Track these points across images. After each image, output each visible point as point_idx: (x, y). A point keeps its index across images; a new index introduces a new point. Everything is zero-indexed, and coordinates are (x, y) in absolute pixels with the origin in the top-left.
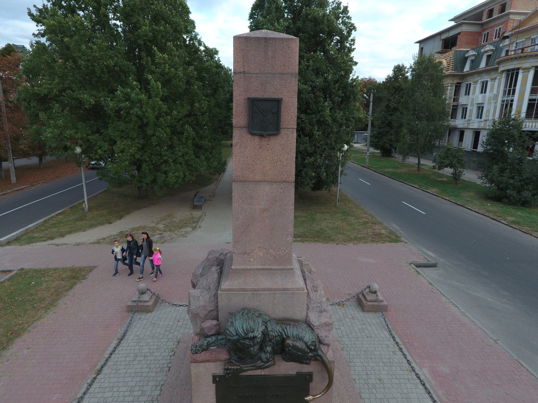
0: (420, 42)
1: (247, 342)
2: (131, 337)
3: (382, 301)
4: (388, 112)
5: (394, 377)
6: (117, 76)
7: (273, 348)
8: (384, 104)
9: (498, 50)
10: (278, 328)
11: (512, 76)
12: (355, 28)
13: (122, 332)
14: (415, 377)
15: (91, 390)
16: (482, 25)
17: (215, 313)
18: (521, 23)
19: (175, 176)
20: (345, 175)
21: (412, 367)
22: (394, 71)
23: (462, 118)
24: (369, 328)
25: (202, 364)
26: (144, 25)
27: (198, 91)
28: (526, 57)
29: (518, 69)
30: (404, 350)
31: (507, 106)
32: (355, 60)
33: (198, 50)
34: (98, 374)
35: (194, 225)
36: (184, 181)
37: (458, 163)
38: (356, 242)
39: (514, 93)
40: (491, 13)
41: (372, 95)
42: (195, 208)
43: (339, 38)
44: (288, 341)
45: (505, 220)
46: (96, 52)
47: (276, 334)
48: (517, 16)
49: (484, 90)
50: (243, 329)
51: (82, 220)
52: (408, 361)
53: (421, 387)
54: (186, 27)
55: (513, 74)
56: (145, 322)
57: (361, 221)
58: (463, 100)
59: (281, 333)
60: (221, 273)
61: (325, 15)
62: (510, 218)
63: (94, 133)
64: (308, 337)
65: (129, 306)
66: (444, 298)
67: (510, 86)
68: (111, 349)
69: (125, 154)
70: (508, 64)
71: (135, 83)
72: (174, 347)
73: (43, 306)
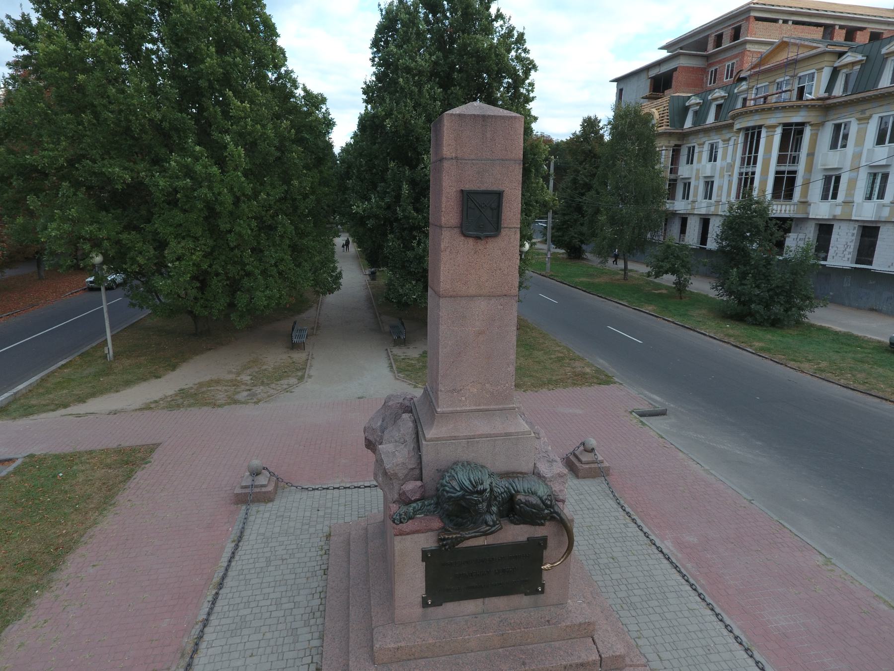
0: (618, 80)
1: (475, 497)
2: (253, 537)
3: (602, 462)
4: (576, 189)
5: (630, 553)
6: (167, 137)
7: (498, 508)
8: (568, 179)
9: (731, 98)
10: (504, 483)
11: (752, 136)
12: (535, 67)
13: (234, 533)
14: (656, 551)
15: (217, 609)
16: (707, 57)
17: (417, 472)
18: (763, 59)
19: (265, 296)
20: (526, 288)
21: (651, 540)
22: (583, 125)
23: (683, 198)
24: (589, 499)
25: (409, 537)
26: (208, 56)
27: (297, 161)
28: (770, 109)
29: (760, 127)
30: (639, 522)
31: (747, 181)
32: (533, 113)
33: (292, 95)
34: (221, 588)
35: (300, 374)
36: (278, 304)
37: (683, 266)
38: (551, 387)
39: (755, 163)
40: (719, 39)
42: (294, 346)
43: (510, 81)
44: (519, 497)
45: (751, 346)
46: (132, 97)
47: (502, 490)
48: (756, 46)
49: (713, 158)
50: (470, 481)
51: (107, 375)
52: (645, 533)
53: (666, 561)
54: (274, 58)
55: (753, 134)
56: (267, 515)
57: (553, 356)
58: (684, 171)
59: (508, 488)
60: (416, 422)
61: (492, 45)
62: (757, 344)
63: (129, 227)
64: (542, 491)
65: (237, 495)
66: (681, 454)
67: (750, 153)
68: (226, 555)
69: (183, 262)
70: (746, 119)
71: (198, 148)
72: (322, 543)
73: (93, 506)
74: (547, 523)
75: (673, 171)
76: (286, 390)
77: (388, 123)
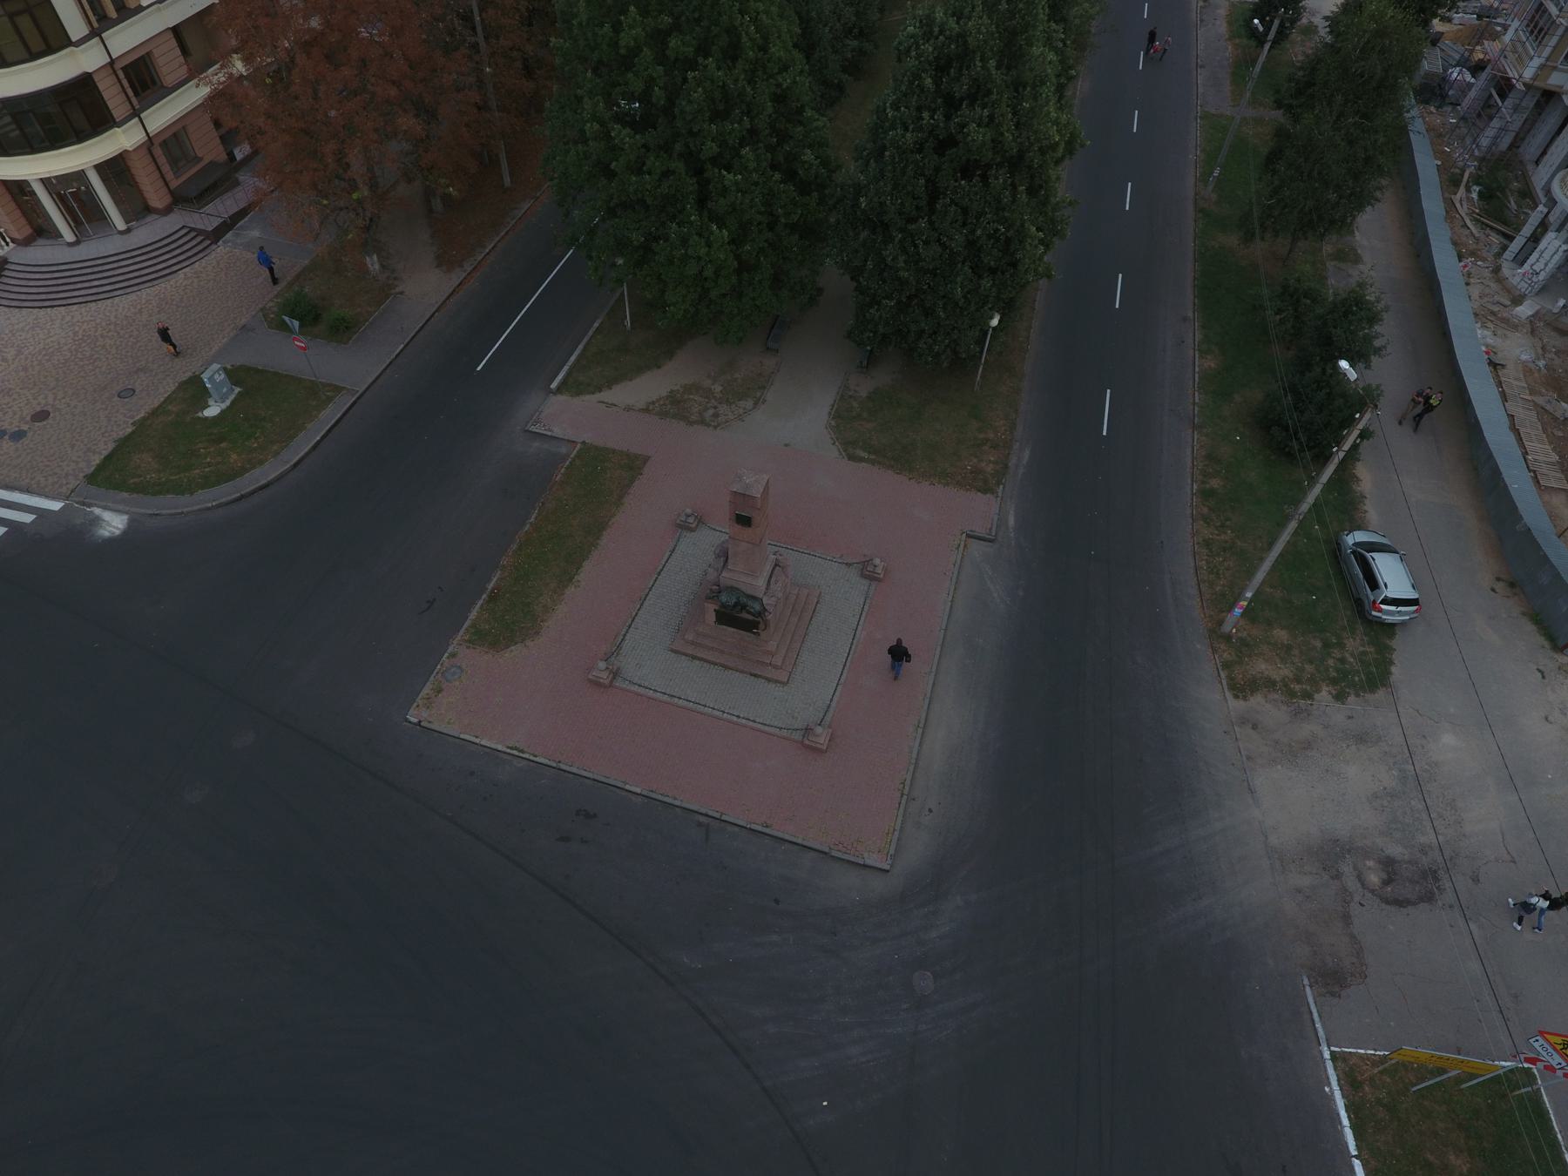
41: (1277, 22)
57: (982, 436)
62: (1215, 483)
64: (757, 607)
76: (740, 418)
77: (863, 201)
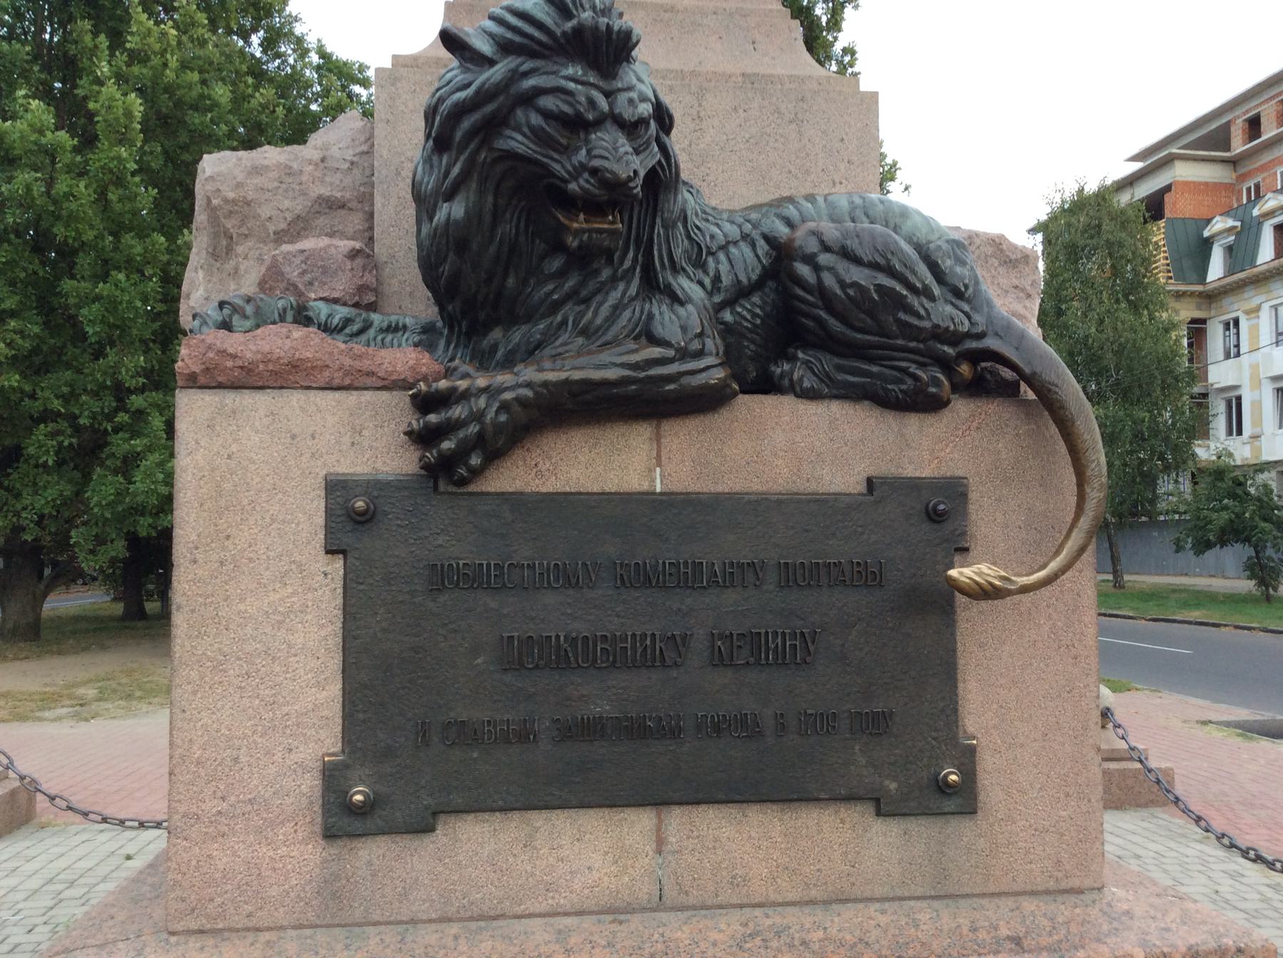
16: (1234, 163)
17: (355, 222)
23: (1230, 433)
25: (262, 401)
37: (1265, 520)
40: (1254, 125)
47: (733, 232)
58: (1220, 374)
74: (961, 408)
75: (1198, 372)
